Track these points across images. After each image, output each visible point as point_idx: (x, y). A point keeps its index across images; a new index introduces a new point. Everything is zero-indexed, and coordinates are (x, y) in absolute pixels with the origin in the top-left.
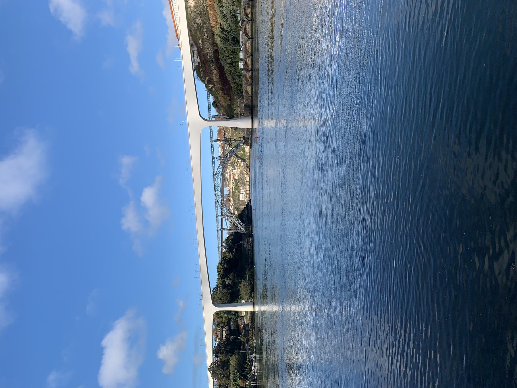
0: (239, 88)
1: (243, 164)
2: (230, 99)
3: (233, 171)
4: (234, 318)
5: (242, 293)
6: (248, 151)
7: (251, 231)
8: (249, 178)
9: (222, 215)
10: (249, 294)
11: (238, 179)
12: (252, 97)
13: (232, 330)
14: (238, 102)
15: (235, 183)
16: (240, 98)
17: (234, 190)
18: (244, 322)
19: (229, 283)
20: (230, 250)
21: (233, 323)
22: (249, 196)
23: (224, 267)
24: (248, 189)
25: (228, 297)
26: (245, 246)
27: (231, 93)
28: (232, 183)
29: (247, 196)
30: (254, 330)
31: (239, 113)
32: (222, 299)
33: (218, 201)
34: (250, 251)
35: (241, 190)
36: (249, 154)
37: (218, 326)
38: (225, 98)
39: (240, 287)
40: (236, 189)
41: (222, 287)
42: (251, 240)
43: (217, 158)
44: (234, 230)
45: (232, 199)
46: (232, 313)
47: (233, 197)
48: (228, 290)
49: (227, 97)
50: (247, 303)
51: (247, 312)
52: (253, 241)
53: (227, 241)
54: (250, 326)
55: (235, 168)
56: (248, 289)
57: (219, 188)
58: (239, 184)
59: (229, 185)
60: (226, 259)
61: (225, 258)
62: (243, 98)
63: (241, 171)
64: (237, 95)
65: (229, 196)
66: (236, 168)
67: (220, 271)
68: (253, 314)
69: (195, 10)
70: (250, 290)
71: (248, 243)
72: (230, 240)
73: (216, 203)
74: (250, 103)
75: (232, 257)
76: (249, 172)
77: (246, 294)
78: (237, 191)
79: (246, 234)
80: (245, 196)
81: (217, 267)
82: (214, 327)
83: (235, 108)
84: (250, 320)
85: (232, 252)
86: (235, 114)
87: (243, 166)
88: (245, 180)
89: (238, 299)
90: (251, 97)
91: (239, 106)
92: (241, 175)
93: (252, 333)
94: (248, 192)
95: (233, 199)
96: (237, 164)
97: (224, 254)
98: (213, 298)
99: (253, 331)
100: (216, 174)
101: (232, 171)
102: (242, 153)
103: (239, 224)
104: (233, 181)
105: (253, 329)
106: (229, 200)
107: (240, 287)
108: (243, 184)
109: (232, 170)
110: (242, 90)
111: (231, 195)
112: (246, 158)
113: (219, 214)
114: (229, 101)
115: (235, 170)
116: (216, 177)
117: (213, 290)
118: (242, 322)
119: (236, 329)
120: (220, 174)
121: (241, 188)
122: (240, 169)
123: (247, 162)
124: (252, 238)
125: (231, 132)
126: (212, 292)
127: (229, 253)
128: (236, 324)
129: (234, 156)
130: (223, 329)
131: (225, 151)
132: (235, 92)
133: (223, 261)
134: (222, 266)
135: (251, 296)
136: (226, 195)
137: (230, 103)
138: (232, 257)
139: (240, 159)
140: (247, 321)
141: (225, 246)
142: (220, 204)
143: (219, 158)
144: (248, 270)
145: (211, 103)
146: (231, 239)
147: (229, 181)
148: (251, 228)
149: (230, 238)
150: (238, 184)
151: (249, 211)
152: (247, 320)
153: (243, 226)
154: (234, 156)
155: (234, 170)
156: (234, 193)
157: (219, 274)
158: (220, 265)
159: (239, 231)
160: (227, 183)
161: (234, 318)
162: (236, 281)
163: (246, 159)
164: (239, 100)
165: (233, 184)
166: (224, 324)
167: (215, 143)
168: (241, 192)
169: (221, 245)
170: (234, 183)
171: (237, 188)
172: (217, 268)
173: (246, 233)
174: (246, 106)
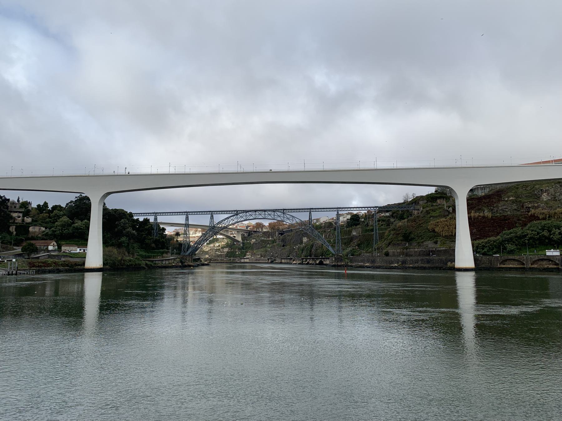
1: (220, 254)
13: (29, 228)
21: (44, 232)
34: (160, 262)
36: (238, 262)
46: (65, 230)
69: (559, 193)
81: (123, 210)
112: (232, 258)
116: (279, 214)
119: (30, 236)
122: (210, 250)
125: (265, 239)
129: (229, 242)
131: (237, 232)
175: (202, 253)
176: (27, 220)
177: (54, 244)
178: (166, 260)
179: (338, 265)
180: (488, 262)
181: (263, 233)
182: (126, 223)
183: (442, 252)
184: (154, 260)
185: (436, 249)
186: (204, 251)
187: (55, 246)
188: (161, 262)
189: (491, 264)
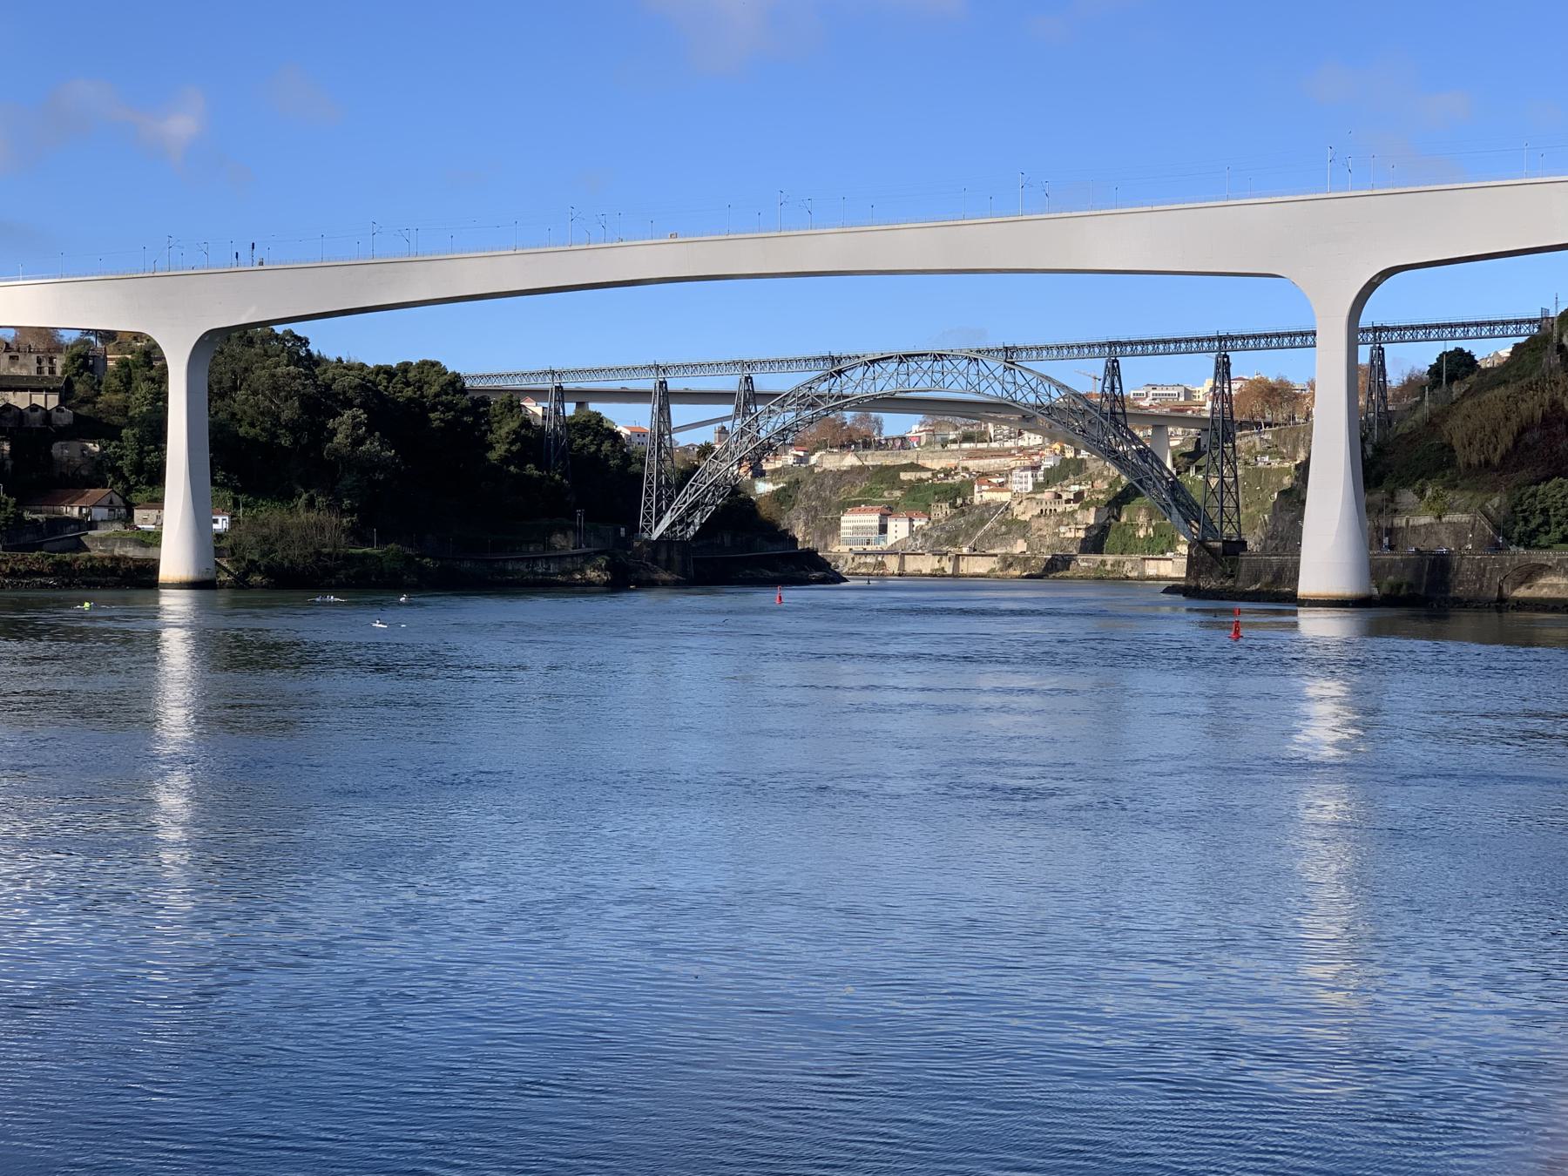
0: (1559, 524)
1: (1069, 535)
2: (1488, 463)
3: (1029, 473)
4: (120, 463)
5: (272, 515)
6: (1152, 568)
7: (644, 576)
8: (982, 570)
9: (751, 398)
10: (263, 555)
11: (977, 500)
12: (1502, 604)
14: (1465, 518)
15: (952, 487)
16: (1497, 528)
17: (904, 476)
18: (93, 525)
19: (334, 432)
20: (531, 440)
21: (92, 457)
22: (864, 570)
23: (434, 409)
24: (912, 565)
25: (252, 425)
26: (558, 540)
27: (1525, 474)
28: (952, 462)
29: (870, 560)
30: (44, 586)
31: (1400, 522)
32: (235, 388)
33: (840, 372)
34: (523, 567)
35: (908, 523)
36: (1134, 574)
37: (73, 360)
38: (1495, 432)
39: (310, 504)
40: (914, 488)
41: (311, 390)
42: (592, 574)
43: (1113, 371)
44: (659, 473)
45: (850, 460)
46: (149, 453)
47: (863, 469)
48: (293, 427)
49: (1501, 448)
50: (214, 547)
51: (158, 545)
52: (587, 588)
53: (588, 427)
54: (68, 557)
55: (1047, 483)
56: (293, 554)
57: (921, 386)
58: (942, 511)
59: (938, 447)
60: (478, 416)
61: (486, 413)
62: (1497, 548)
63: (1026, 525)
64: (1514, 512)
65: (867, 445)
66: (1047, 495)
67: (408, 384)
68: (144, 577)
70: (286, 564)
71: (572, 556)
72: (593, 448)
73: (829, 364)
74: (1458, 591)
75: (493, 456)
76: (1018, 573)
77: (265, 539)
78: (898, 493)
79: (630, 546)
80: (869, 548)
81: (434, 364)
82: (69, 338)
83: (1429, 493)
84: (103, 559)
85: (519, 458)
86: (1392, 495)
87: (1059, 533)
88: (965, 550)
89: (237, 491)
90: (1502, 600)
91: (1444, 520)
92: (998, 522)
93: (30, 573)
94: (892, 564)
95: (853, 468)
96: (1068, 501)
97: (511, 410)
98: (244, 333)
99: (40, 573)
100: (1010, 365)
101: (1025, 469)
102: (1142, 533)
103: (695, 506)
104: (966, 469)
105: (50, 575)
106: (842, 446)
107: (310, 504)
108: (944, 536)
109: (1035, 468)
110: (1543, 540)
111: (874, 459)
112: (1110, 559)
113: (763, 383)
114: (1474, 460)
115: (1036, 485)
116: (992, 365)
117: (290, 333)
118: (93, 510)
120: (1009, 387)
121: (917, 523)
122: (1039, 516)
123: (1085, 562)
124: (607, 584)
125: (1275, 464)
126: (279, 329)
127: (517, 436)
128: (84, 473)
129: (1124, 479)
130: (54, 390)
131: (1155, 427)
132: (1534, 495)
133: (465, 402)
134: (437, 395)
135: (253, 567)
136: (878, 423)
137: (1461, 461)
138: (493, 456)
139: (1101, 522)
140: (103, 540)
141: (557, 412)
142: (823, 388)
143: (1113, 388)
144: (409, 552)
145: (1466, 346)
146: (599, 450)
147: (966, 446)
148: (666, 576)
149: (606, 446)
150: (945, 506)
151: (773, 570)
152: (104, 542)
153: (678, 528)
154: (1124, 479)
155: (1030, 480)
156: (887, 475)
157: (388, 372)
158: (443, 380)
159: (648, 502)
160: (952, 437)
161: (120, 463)
162: (348, 481)
163: (1099, 558)
164: (1484, 522)
165: (947, 473)
166: (84, 401)
167: (1206, 363)
168: (891, 524)
169: (566, 386)
170: (950, 481)
171: (920, 496)
172: (424, 363)
173: (636, 544)
174: (1439, 567)
175: (1008, 533)
176: (60, 419)
177: (111, 502)
178: (548, 559)
179: (1197, 588)
180: (1477, 576)
181: (1274, 433)
182: (360, 423)
183: (1423, 530)
184: (498, 560)
185: (1408, 522)
186: (1015, 521)
187: (118, 507)
188: (528, 567)
189: (1481, 586)
